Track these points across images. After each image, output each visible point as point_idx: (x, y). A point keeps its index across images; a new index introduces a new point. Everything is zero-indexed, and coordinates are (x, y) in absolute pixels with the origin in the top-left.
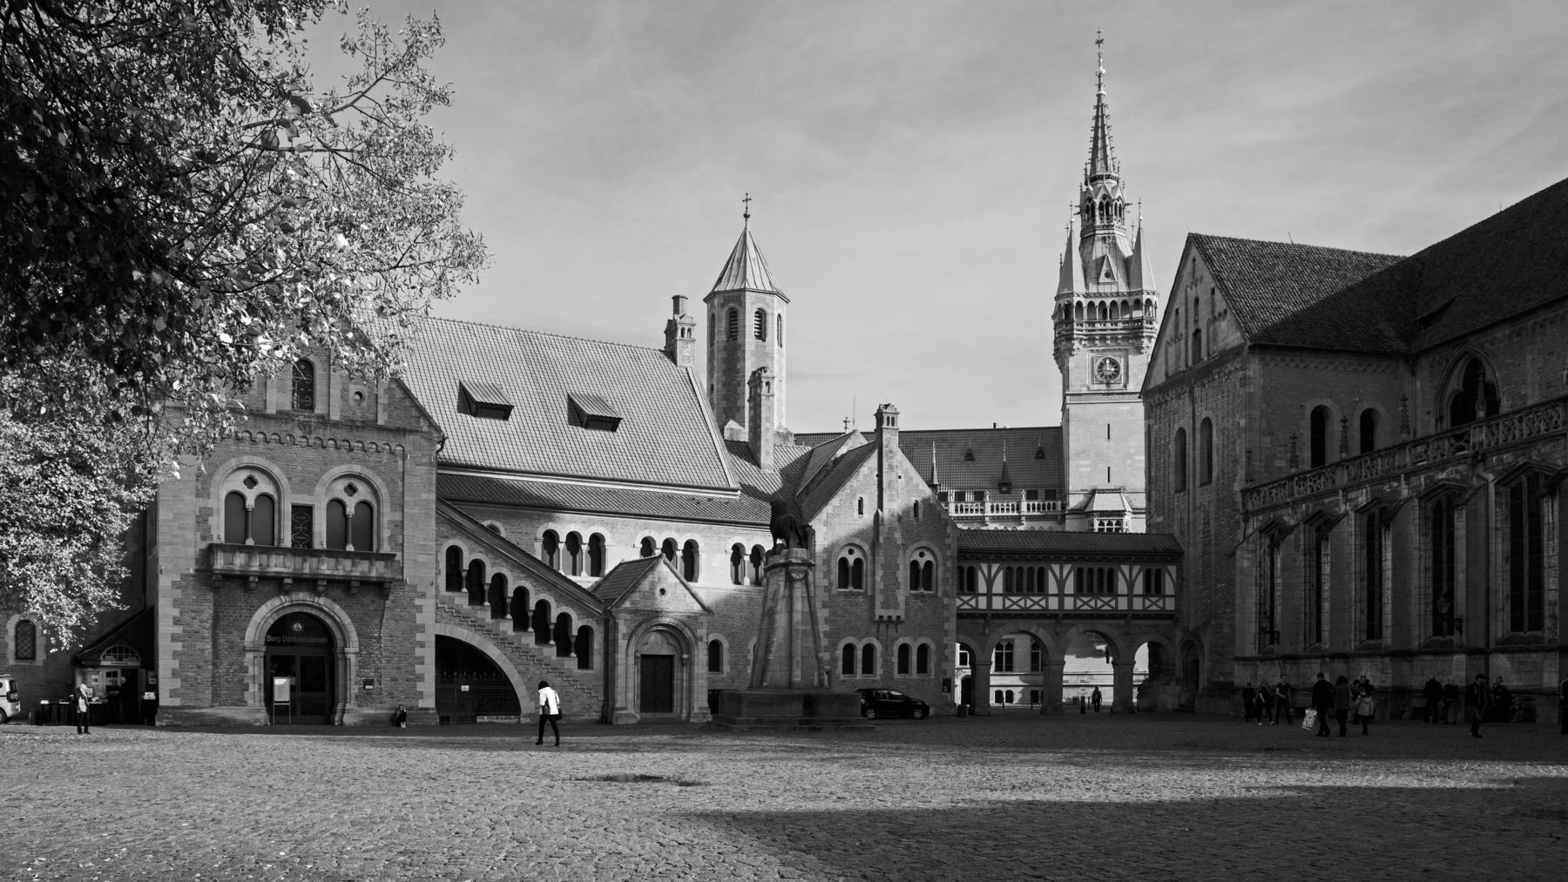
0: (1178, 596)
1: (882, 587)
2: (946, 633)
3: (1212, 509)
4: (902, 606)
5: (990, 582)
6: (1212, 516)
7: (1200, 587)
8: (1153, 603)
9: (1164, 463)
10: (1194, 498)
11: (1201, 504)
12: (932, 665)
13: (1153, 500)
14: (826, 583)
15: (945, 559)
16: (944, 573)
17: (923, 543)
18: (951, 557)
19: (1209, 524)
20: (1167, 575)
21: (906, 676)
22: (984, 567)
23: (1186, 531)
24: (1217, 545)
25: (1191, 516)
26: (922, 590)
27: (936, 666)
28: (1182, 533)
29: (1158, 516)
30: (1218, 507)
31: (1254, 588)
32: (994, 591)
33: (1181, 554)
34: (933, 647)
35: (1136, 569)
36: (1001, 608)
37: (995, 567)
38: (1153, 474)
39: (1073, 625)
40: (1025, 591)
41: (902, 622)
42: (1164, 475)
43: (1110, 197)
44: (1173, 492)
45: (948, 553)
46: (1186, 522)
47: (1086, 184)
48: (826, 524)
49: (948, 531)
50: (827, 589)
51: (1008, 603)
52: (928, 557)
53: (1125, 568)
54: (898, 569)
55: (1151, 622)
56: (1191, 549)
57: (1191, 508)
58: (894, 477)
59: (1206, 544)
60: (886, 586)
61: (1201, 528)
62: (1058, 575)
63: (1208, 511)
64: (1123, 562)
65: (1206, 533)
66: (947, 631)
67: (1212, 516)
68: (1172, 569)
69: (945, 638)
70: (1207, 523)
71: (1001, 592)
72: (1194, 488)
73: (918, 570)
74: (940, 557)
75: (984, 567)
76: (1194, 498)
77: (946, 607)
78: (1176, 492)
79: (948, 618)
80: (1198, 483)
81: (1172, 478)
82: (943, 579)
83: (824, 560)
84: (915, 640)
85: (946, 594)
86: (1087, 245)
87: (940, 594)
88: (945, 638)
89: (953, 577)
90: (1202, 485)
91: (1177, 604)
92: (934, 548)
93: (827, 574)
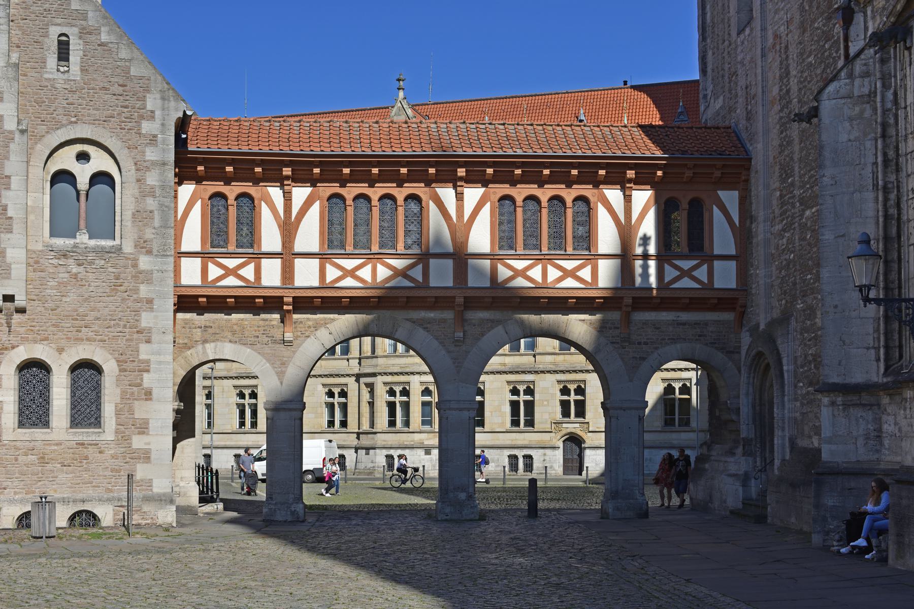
0: (743, 258)
2: (146, 336)
4: (19, 270)
5: (289, 229)
8: (684, 273)
12: (108, 410)
15: (141, 167)
20: (716, 210)
21: (38, 433)
26: (83, 238)
27: (118, 413)
30: (803, 28)
32: (298, 247)
33: (745, 163)
34: (110, 367)
36: (316, 283)
37: (300, 193)
39: (498, 322)
40: (375, 249)
41: (21, 311)
45: (151, 154)
49: (149, 107)
51: (332, 273)
52: (100, 162)
55: (685, 316)
62: (452, 211)
64: (609, 181)
66: (149, 330)
68: (730, 198)
69: (143, 347)
71: (316, 249)
73: (78, 193)
77: (146, 277)
79: (150, 301)
82: (136, 214)
84: (60, 350)
85: (143, 246)
87: (128, 248)
88: (143, 347)
91: (743, 274)
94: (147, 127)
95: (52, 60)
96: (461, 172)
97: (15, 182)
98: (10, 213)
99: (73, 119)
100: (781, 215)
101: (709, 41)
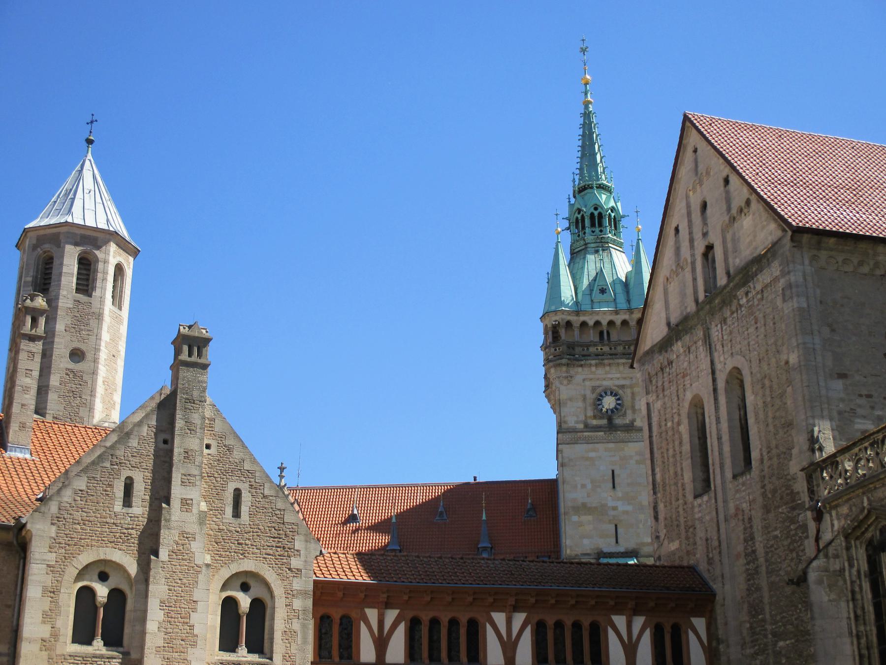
1: (161, 643)
3: (757, 515)
6: (757, 524)
7: (749, 651)
9: (674, 456)
10: (725, 501)
11: (737, 509)
13: (661, 517)
14: (45, 631)
15: (290, 594)
16: (289, 620)
17: (248, 565)
18: (303, 593)
19: (752, 538)
22: (372, 614)
23: (717, 558)
24: (769, 573)
25: (722, 531)
28: (710, 561)
29: (671, 540)
31: (847, 640)
33: (711, 596)
35: (639, 622)
38: (658, 477)
42: (676, 473)
43: (602, 208)
44: (690, 497)
46: (716, 543)
47: (574, 197)
48: (56, 520)
50: (46, 644)
53: (620, 621)
54: (194, 610)
56: (727, 587)
57: (721, 517)
58: (193, 443)
59: (752, 575)
60: (169, 642)
61: (740, 548)
63: (750, 519)
65: (751, 555)
67: (757, 524)
68: (700, 623)
70: (750, 538)
72: (723, 482)
74: (278, 590)
75: (372, 614)
76: (725, 501)
78: (696, 497)
80: (729, 475)
81: (688, 476)
83: (45, 590)
86: (578, 260)
89: (304, 626)
90: (735, 477)
92: (270, 576)
93: (48, 617)
94: (295, 563)
95: (229, 510)
96: (512, 600)
97: (200, 606)
98: (196, 632)
99: (241, 557)
100: (752, 642)
101: (659, 495)
